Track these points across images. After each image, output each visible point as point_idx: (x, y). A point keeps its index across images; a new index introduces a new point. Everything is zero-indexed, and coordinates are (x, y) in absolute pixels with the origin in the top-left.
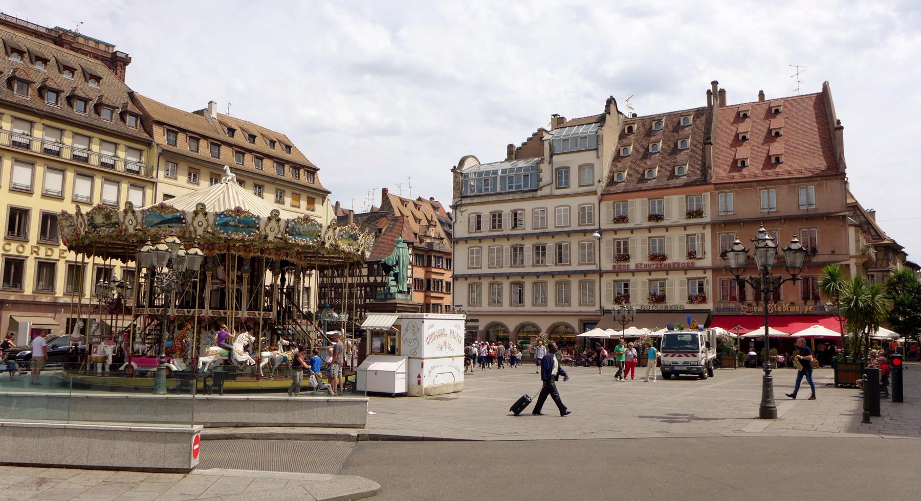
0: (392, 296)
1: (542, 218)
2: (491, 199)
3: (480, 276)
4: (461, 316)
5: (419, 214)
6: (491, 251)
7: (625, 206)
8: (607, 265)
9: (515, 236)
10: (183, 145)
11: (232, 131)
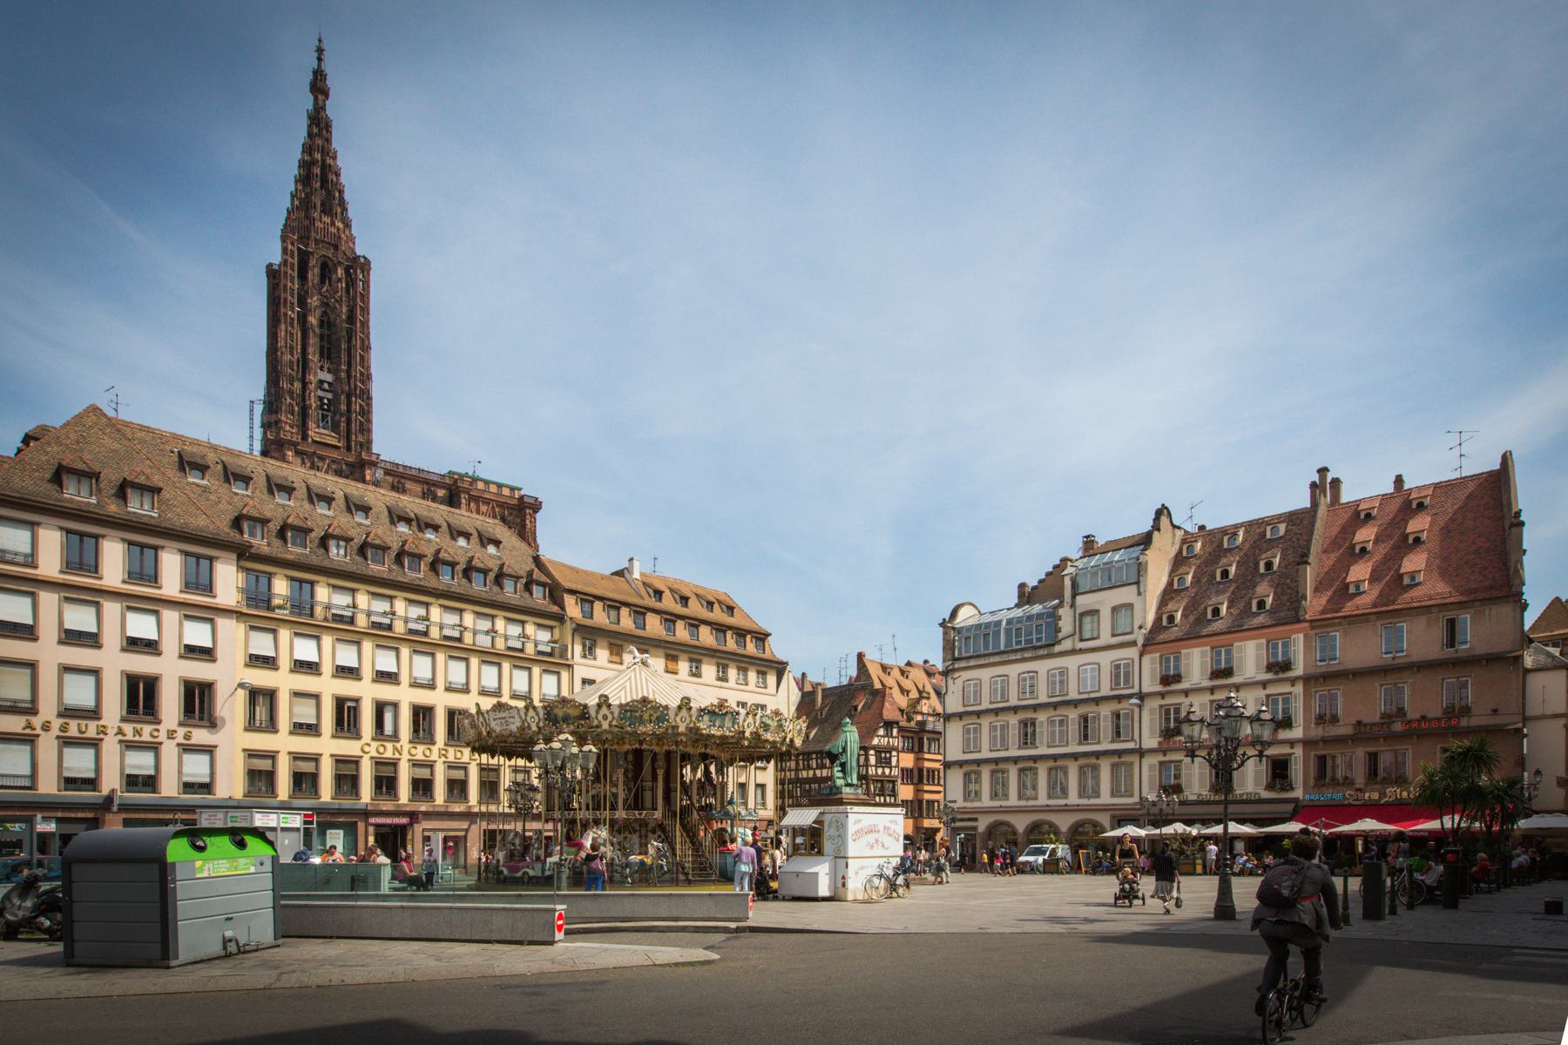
0: (838, 790)
1: (1061, 682)
2: (992, 660)
3: (979, 762)
4: (898, 810)
5: (907, 684)
6: (993, 728)
7: (1177, 659)
8: (1151, 742)
9: (1025, 708)
10: (600, 617)
11: (659, 594)
